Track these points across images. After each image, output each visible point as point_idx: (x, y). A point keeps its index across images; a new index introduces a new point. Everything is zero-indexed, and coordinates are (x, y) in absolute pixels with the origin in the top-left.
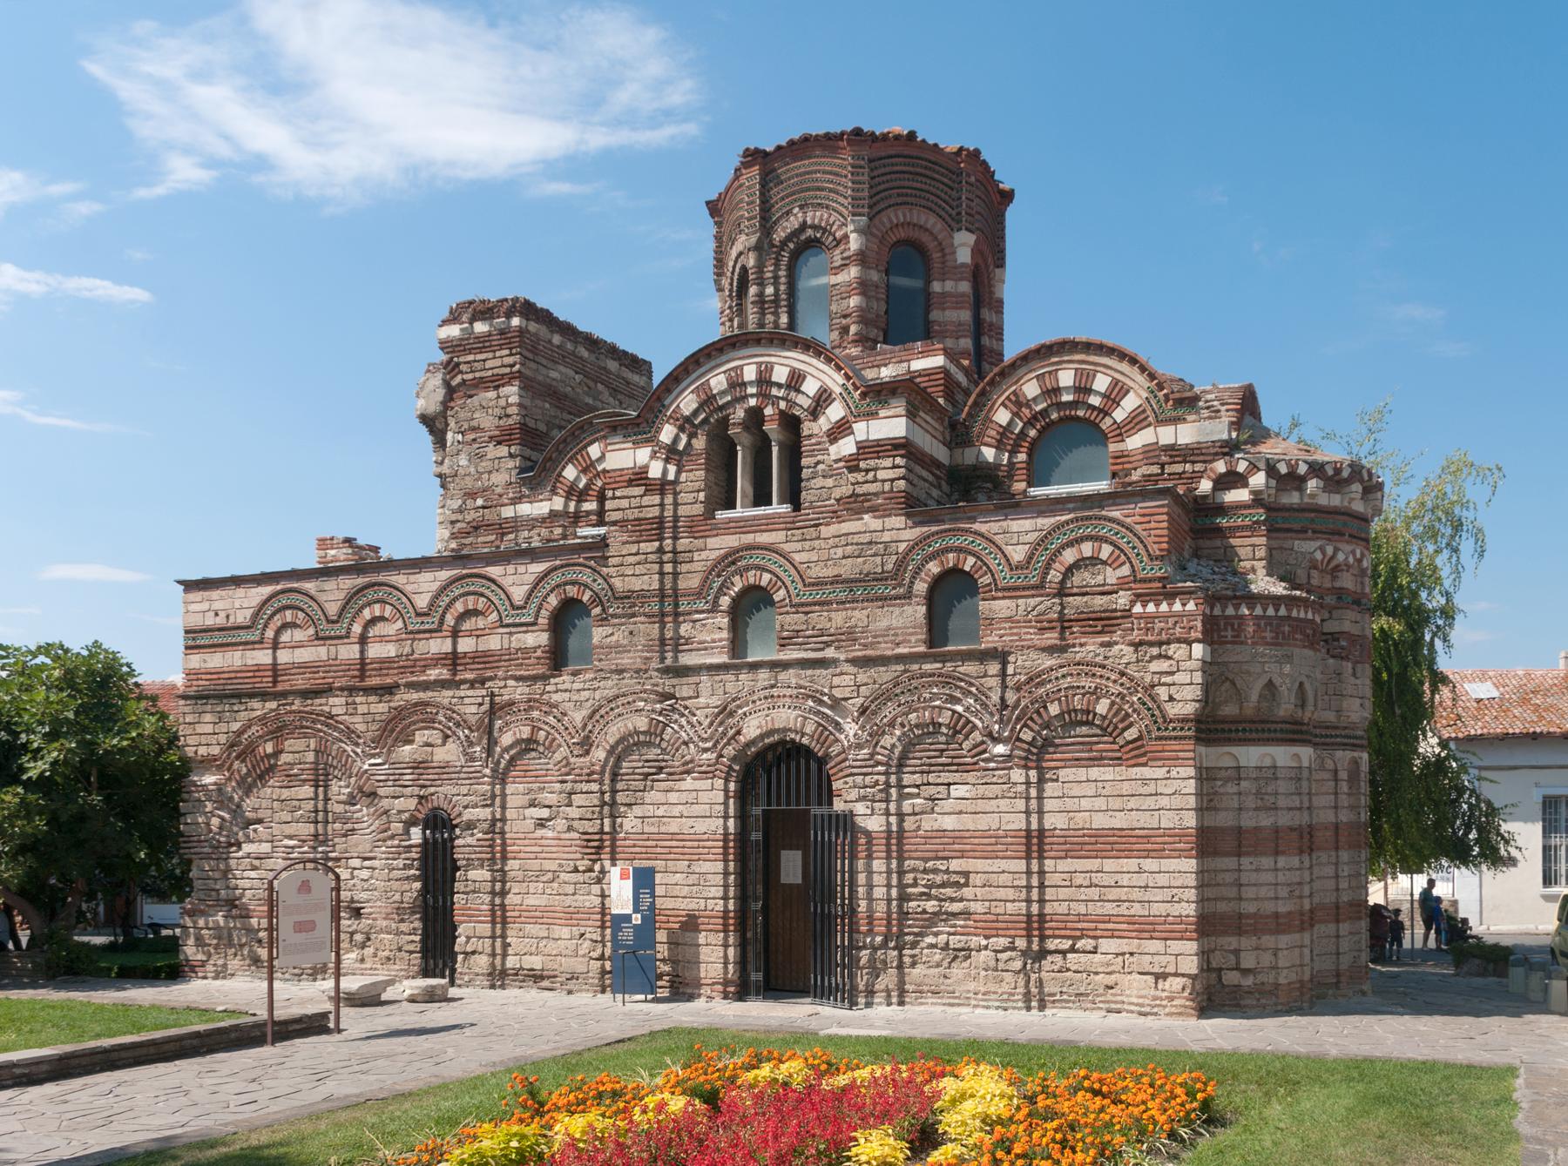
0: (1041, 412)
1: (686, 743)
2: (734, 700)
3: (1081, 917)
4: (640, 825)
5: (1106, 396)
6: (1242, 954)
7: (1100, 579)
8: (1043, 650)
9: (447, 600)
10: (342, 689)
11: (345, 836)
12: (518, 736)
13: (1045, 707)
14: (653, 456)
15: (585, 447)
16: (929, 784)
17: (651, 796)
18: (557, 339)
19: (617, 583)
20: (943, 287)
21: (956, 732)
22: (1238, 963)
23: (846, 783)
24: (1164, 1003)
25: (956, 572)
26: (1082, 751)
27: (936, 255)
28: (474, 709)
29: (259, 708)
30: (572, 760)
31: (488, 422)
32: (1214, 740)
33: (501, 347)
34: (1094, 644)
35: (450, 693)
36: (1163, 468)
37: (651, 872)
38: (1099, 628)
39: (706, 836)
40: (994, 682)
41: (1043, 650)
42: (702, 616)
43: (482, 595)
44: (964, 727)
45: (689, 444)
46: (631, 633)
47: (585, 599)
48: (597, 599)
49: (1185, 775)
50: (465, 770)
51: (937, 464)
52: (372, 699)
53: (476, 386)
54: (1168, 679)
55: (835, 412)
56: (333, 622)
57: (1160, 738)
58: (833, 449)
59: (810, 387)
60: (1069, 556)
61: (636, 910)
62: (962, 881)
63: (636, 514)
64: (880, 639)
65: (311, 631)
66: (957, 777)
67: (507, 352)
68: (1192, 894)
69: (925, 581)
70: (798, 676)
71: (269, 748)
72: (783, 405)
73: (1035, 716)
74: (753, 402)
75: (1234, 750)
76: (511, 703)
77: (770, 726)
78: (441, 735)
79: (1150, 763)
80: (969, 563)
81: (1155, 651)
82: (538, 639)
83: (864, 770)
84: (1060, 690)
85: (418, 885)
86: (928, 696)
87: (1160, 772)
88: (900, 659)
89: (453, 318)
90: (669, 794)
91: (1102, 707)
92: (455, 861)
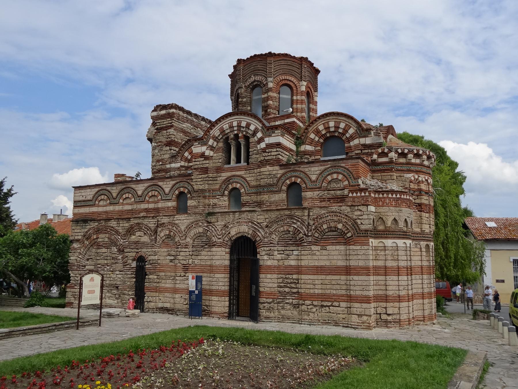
0: (324, 135)
1: (214, 236)
2: (229, 223)
3: (334, 295)
4: (200, 262)
5: (344, 129)
6: (388, 309)
7: (339, 185)
8: (321, 207)
13: (322, 226)
14: (207, 149)
16: (287, 250)
17: (203, 253)
18: (185, 115)
19: (195, 187)
20: (297, 98)
21: (295, 234)
22: (386, 312)
23: (261, 249)
24: (361, 324)
25: (294, 184)
26: (334, 240)
27: (294, 88)
28: (153, 225)
30: (180, 241)
31: (164, 140)
32: (377, 237)
33: (168, 118)
34: (337, 206)
35: (147, 220)
36: (362, 151)
37: (201, 277)
38: (339, 201)
39: (219, 266)
40: (306, 218)
41: (321, 207)
42: (219, 197)
43: (157, 191)
44: (297, 232)
45: (217, 145)
47: (186, 191)
48: (189, 192)
49: (366, 249)
51: (291, 150)
52: (124, 222)
53: (161, 129)
54: (360, 218)
55: (259, 135)
57: (358, 236)
58: (258, 146)
59: (252, 128)
60: (329, 178)
61: (196, 289)
62: (297, 282)
64: (272, 204)
65: (108, 201)
66: (295, 248)
67: (170, 119)
69: (285, 186)
70: (247, 215)
72: (244, 133)
73: (319, 229)
74: (236, 132)
75: (383, 241)
76: (164, 224)
77: (239, 232)
78: (143, 233)
79: (355, 244)
80: (299, 181)
81: (356, 208)
82: (172, 204)
83: (266, 245)
84: (327, 221)
85: (134, 280)
86: (286, 222)
87: (359, 247)
88: (278, 210)
89: (155, 110)
90: (209, 252)
91: (340, 226)
92: (146, 272)
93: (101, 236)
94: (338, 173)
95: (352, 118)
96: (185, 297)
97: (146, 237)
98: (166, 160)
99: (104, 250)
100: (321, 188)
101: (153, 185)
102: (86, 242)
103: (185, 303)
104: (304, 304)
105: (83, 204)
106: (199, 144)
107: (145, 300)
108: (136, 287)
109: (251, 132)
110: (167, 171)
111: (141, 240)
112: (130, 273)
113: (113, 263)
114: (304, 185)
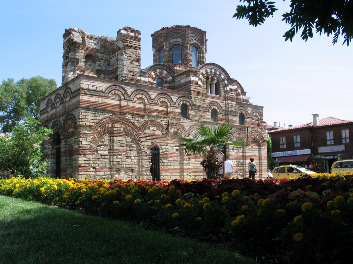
9: (158, 98)
10: (132, 113)
11: (130, 151)
12: (174, 131)
15: (156, 69)
19: (194, 102)
29: (106, 115)
40: (246, 132)
43: (166, 98)
46: (197, 113)
47: (188, 104)
50: (162, 137)
56: (129, 96)
58: (225, 88)
59: (222, 76)
63: (196, 90)
68: (267, 166)
71: (110, 125)
74: (213, 76)
78: (156, 128)
80: (244, 112)
85: (151, 163)
89: (125, 29)
91: (258, 137)
93: (116, 125)
94: (257, 112)
95: (240, 85)
96: (190, 175)
97: (158, 131)
98: (136, 72)
99: (120, 138)
100: (251, 118)
101: (163, 93)
102: (99, 129)
103: (190, 178)
104: (247, 174)
105: (93, 93)
106: (194, 74)
107: (161, 178)
108: (151, 169)
109: (221, 79)
110: (137, 80)
111: (156, 133)
112: (147, 158)
113: (127, 150)
114: (246, 115)
